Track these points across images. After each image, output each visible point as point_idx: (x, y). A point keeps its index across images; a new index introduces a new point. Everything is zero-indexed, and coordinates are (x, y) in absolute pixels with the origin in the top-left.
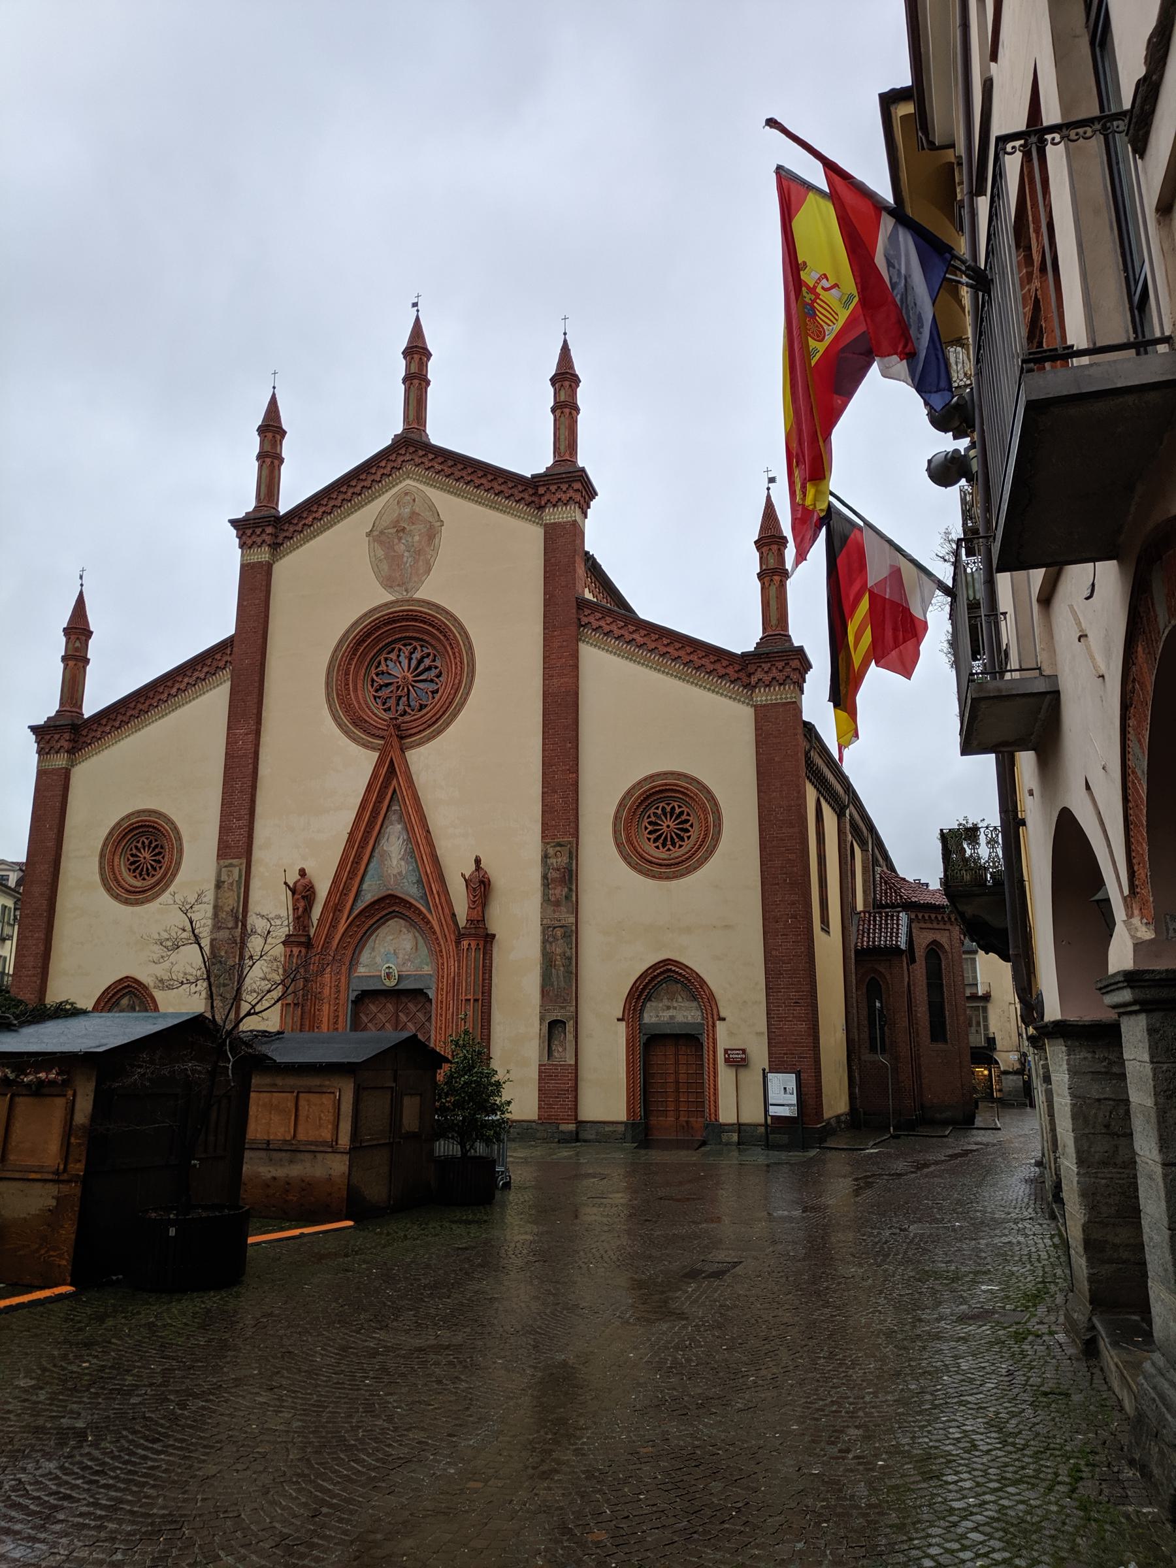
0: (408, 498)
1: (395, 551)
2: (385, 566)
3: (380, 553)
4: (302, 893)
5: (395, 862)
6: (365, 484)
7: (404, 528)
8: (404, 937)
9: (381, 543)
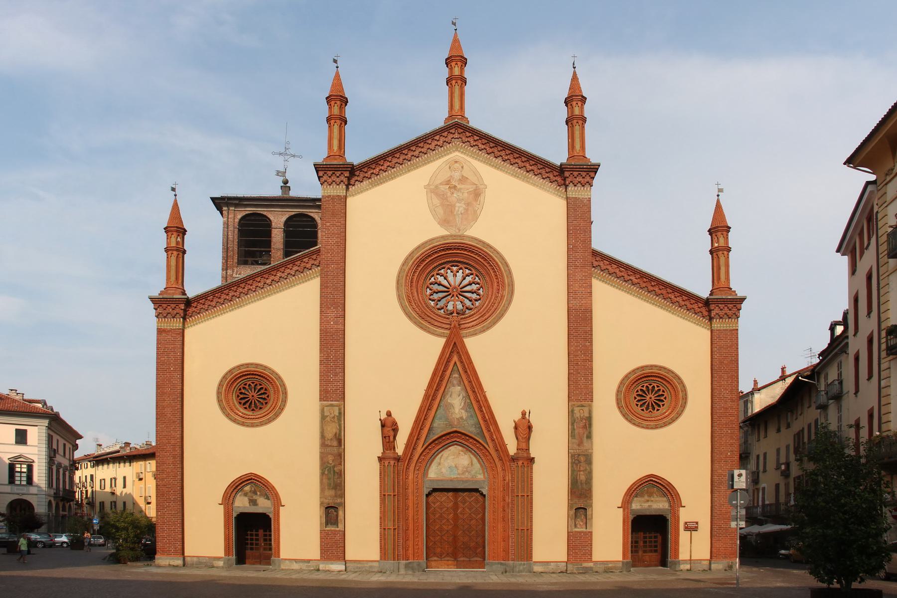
0: (457, 165)
1: (448, 201)
2: (440, 211)
3: (436, 201)
4: (389, 427)
5: (457, 411)
6: (422, 150)
7: (455, 187)
8: (462, 457)
9: (437, 195)
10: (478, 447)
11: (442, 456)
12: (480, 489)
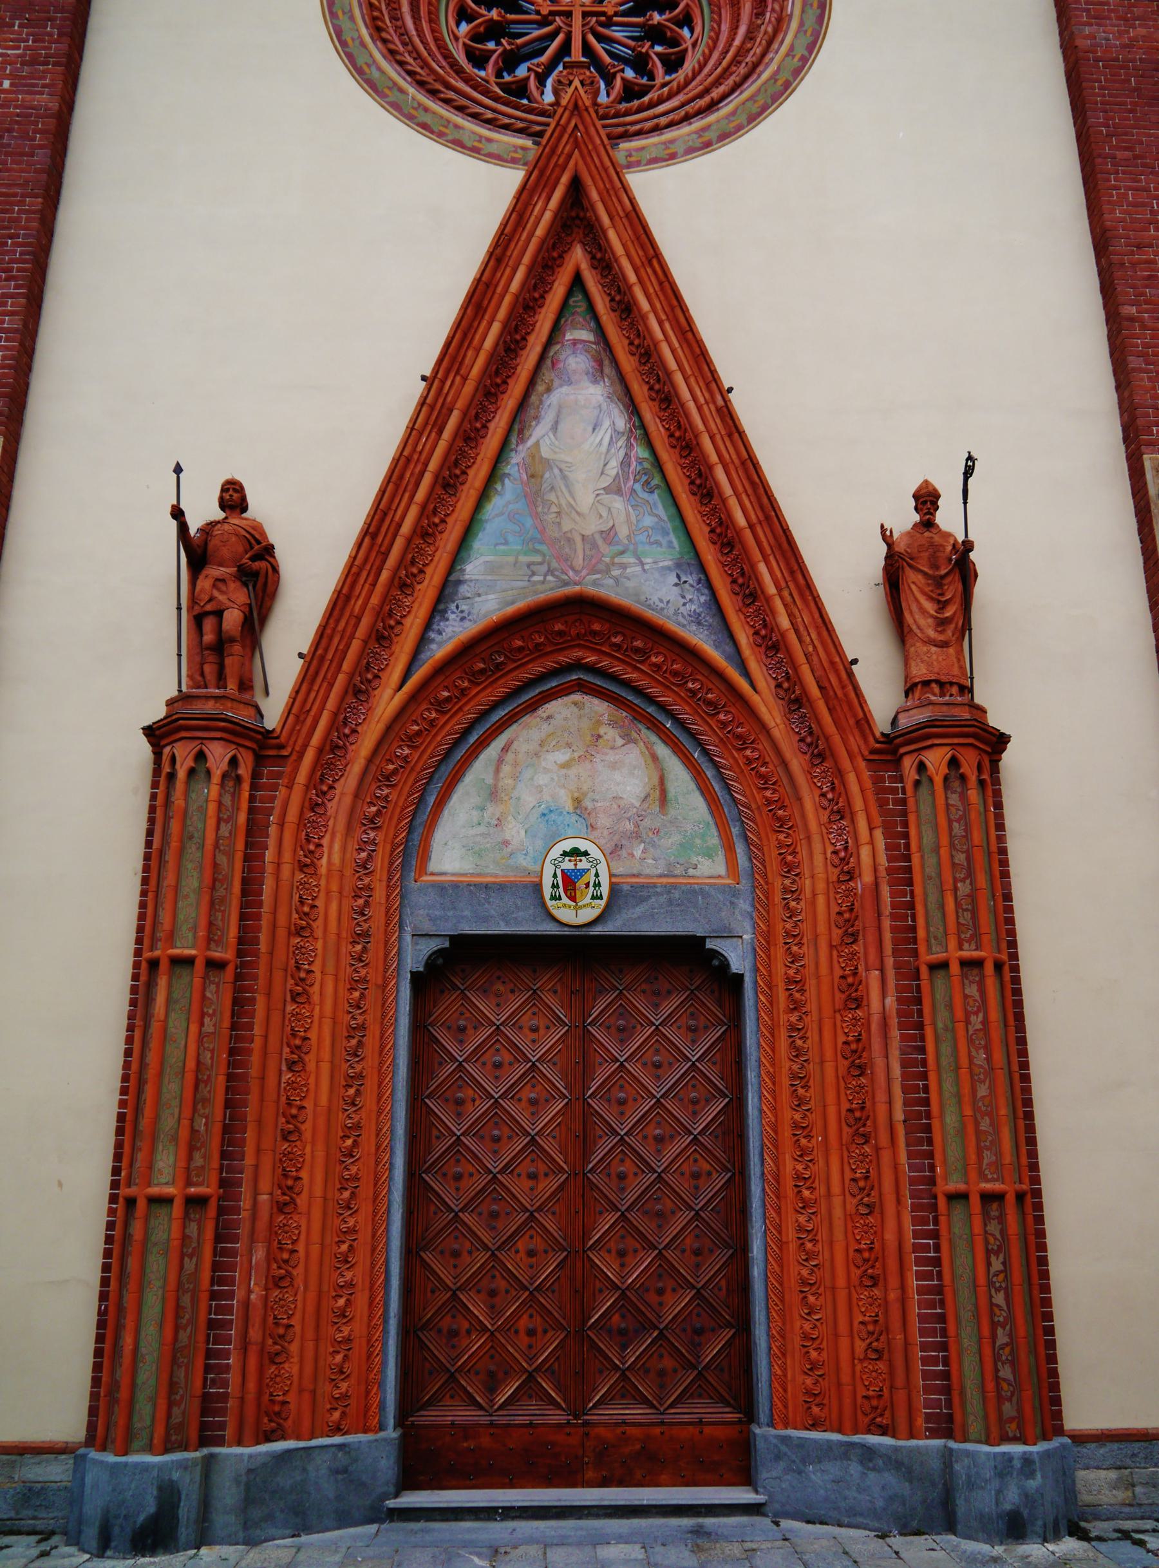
8: (611, 757)
10: (693, 692)
11: (506, 749)
12: (710, 944)
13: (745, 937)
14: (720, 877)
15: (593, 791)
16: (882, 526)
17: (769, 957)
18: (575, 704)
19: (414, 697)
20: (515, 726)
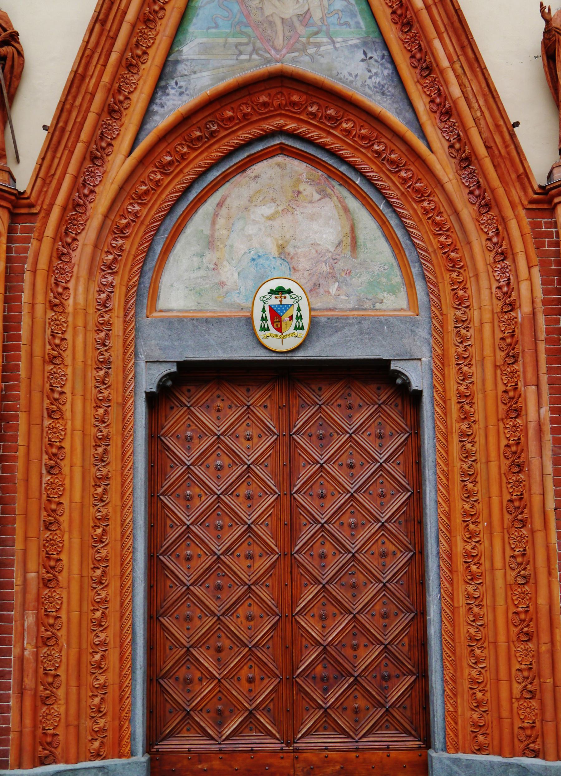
8: (310, 209)
10: (378, 154)
11: (220, 205)
12: (394, 366)
13: (423, 359)
14: (402, 309)
15: (295, 239)
16: (541, 4)
17: (443, 376)
18: (278, 165)
19: (142, 161)
20: (227, 185)
